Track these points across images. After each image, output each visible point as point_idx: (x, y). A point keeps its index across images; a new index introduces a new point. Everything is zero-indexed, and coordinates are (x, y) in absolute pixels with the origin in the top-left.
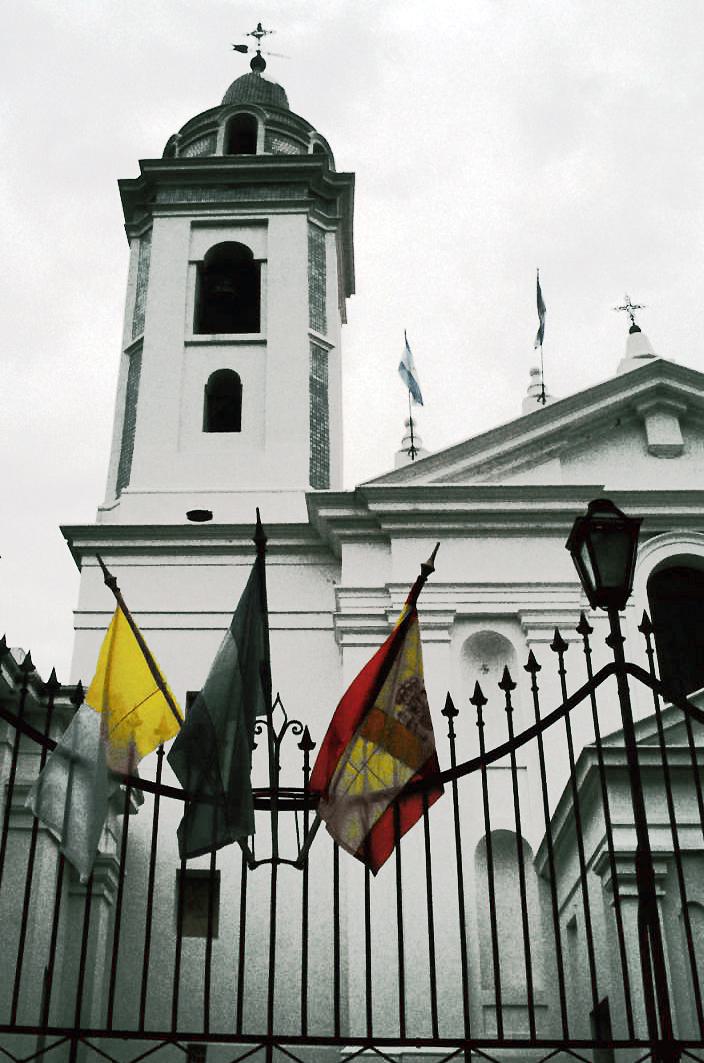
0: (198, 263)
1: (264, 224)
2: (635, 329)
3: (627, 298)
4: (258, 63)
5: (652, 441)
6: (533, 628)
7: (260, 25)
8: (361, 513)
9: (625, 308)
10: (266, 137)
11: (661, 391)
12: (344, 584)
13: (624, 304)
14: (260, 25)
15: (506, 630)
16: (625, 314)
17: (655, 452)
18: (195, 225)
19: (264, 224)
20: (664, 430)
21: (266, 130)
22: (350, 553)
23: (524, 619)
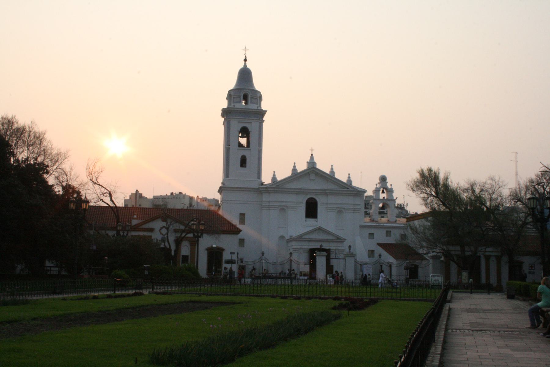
0: (239, 131)
2: (312, 155)
3: (312, 148)
4: (245, 60)
6: (289, 208)
7: (246, 47)
8: (267, 190)
9: (310, 150)
10: (251, 99)
11: (313, 171)
12: (264, 200)
13: (311, 149)
14: (246, 47)
16: (311, 151)
17: (310, 180)
19: (251, 123)
20: (312, 176)
21: (251, 97)
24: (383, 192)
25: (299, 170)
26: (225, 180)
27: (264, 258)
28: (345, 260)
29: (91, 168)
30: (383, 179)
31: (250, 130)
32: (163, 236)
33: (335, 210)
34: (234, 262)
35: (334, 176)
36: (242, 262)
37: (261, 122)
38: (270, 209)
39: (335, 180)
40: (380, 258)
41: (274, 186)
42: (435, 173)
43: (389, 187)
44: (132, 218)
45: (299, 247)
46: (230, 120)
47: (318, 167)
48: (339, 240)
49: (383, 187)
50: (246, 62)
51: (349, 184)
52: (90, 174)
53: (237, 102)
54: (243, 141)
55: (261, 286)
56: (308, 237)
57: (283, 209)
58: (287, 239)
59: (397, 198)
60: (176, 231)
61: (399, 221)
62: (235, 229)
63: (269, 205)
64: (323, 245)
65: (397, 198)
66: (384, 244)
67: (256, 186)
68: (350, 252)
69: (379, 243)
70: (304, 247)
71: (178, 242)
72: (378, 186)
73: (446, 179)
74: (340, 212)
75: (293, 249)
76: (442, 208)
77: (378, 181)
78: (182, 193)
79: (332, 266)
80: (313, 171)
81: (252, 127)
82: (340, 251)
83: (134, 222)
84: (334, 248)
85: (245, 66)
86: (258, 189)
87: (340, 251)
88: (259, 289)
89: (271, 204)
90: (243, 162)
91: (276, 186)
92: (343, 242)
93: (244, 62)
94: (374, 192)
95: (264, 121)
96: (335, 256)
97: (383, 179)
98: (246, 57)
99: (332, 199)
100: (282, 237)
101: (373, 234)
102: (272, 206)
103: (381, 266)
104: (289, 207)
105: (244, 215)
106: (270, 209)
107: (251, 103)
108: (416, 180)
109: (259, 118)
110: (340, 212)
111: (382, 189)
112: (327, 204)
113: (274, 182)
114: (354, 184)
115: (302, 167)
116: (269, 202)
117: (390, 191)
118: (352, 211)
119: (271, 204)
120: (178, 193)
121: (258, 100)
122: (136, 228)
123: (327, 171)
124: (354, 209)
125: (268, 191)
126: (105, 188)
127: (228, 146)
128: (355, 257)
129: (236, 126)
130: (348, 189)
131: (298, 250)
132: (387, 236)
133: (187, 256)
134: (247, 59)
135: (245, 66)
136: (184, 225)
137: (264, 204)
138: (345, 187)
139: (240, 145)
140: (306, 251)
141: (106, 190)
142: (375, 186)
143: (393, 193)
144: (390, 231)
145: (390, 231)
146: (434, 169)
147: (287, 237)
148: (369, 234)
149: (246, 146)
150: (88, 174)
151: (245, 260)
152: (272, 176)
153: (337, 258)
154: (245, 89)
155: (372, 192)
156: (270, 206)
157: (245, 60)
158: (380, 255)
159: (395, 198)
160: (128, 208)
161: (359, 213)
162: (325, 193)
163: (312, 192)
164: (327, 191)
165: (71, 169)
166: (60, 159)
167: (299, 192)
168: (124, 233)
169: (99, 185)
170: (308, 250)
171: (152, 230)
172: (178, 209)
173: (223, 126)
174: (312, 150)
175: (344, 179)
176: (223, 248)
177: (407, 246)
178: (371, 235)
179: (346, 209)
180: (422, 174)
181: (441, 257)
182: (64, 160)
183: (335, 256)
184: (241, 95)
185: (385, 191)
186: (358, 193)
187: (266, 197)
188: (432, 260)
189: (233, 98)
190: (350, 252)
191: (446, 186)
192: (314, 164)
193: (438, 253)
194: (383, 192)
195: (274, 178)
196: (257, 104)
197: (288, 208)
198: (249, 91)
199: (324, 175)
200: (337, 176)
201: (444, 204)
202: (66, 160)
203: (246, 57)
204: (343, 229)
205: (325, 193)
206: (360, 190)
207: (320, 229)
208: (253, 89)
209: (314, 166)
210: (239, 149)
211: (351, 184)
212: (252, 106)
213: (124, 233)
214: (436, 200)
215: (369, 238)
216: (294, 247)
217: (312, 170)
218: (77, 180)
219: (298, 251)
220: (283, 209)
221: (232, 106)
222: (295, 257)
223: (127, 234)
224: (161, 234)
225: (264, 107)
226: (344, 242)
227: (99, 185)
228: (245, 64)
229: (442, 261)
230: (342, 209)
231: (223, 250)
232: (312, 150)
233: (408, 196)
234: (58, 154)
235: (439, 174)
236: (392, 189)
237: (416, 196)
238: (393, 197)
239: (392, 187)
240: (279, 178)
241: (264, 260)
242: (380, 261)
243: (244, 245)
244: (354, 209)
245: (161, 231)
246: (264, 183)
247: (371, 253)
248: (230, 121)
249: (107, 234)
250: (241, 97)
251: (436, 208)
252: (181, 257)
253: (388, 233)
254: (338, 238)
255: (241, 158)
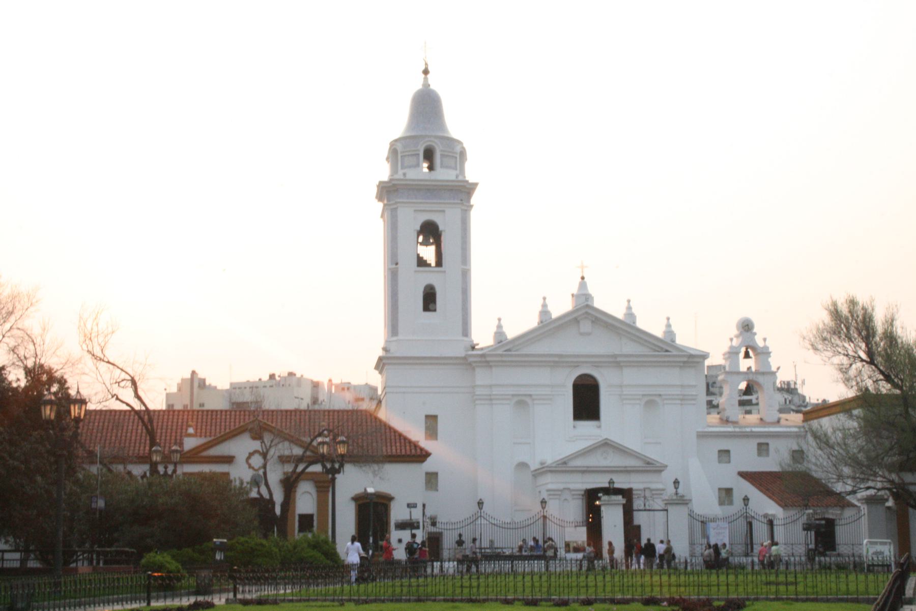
1: (444, 211)
2: (583, 278)
4: (426, 72)
5: (582, 330)
6: (536, 399)
7: (425, 43)
10: (441, 158)
11: (586, 313)
12: (478, 383)
14: (425, 43)
15: (528, 400)
17: (582, 334)
18: (415, 211)
19: (444, 211)
20: (586, 326)
21: (441, 155)
22: (478, 370)
23: (534, 397)
24: (747, 356)
25: (555, 314)
26: (390, 342)
27: (482, 514)
28: (665, 512)
29: (89, 327)
30: (747, 327)
31: (441, 228)
32: (254, 472)
33: (639, 399)
34: (415, 525)
35: (634, 323)
36: (434, 524)
37: (466, 208)
38: (494, 402)
39: (637, 334)
40: (746, 505)
41: (500, 352)
42: (864, 309)
43: (760, 344)
44: (184, 434)
45: (561, 486)
46: (395, 206)
47: (597, 304)
48: (652, 468)
49: (747, 344)
50: (429, 76)
51: (668, 340)
52: (88, 338)
53: (410, 167)
54: (428, 253)
55: (478, 578)
56: (579, 463)
57: (522, 403)
58: (532, 468)
59: (778, 368)
60: (283, 460)
61: (787, 420)
62: (416, 449)
63: (490, 395)
64: (615, 480)
65: (778, 368)
66: (755, 473)
67: (461, 353)
68: (677, 494)
69: (743, 472)
70: (572, 486)
71: (290, 484)
72: (735, 343)
73: (891, 322)
74: (651, 403)
75: (548, 490)
76: (885, 387)
77: (735, 332)
78: (295, 375)
79: (639, 527)
80: (586, 313)
81: (446, 223)
82: (654, 492)
83: (190, 443)
84: (641, 486)
85: (426, 85)
86: (465, 358)
87: (654, 492)
88: (475, 584)
89: (494, 393)
90: (429, 299)
91: (505, 351)
92: (661, 471)
93: (423, 76)
94: (727, 356)
95: (472, 206)
96: (645, 505)
97: (747, 327)
98: (426, 64)
99: (630, 376)
100: (523, 466)
101: (728, 452)
102: (497, 397)
103: (750, 524)
104: (534, 397)
105: (435, 417)
106: (492, 404)
107: (442, 166)
108: (821, 326)
109: (462, 200)
110: (651, 403)
111: (743, 350)
112: (621, 386)
113: (499, 343)
114: (680, 341)
115: (561, 306)
116: (491, 386)
117: (763, 353)
118: (679, 402)
119: (495, 391)
120: (287, 375)
121: (458, 159)
122: (194, 456)
123: (619, 313)
124: (681, 397)
125: (488, 362)
126: (122, 370)
127: (394, 266)
128: (689, 505)
129: (412, 220)
130: (667, 351)
131: (560, 493)
132: (760, 453)
133: (311, 516)
134: (430, 69)
135: (426, 85)
136: (301, 446)
137: (479, 391)
138: (659, 347)
139: (421, 262)
140: (579, 495)
141: (123, 373)
142: (729, 344)
143: (770, 356)
144: (767, 444)
145: (767, 444)
146: (862, 299)
147: (534, 466)
148: (720, 451)
149: (433, 264)
150: (82, 339)
151: (439, 520)
152: (494, 329)
153: (647, 508)
154: (426, 136)
155: (722, 357)
156: (492, 397)
157: (426, 72)
158: (746, 500)
159: (774, 369)
160: (174, 411)
161: (694, 404)
162: (616, 362)
163: (586, 362)
164: (619, 359)
165: (44, 330)
166: (18, 306)
167: (556, 362)
168: (166, 468)
169: (108, 362)
170: (583, 493)
171: (229, 460)
172: (287, 411)
173: (381, 222)
174: (582, 267)
175: (658, 331)
176: (390, 495)
177: (805, 477)
178: (724, 454)
179: (664, 397)
180: (836, 314)
181: (887, 500)
182: (27, 309)
183: (645, 505)
184: (418, 150)
185: (751, 353)
186: (691, 360)
187: (482, 377)
188: (866, 507)
189: (401, 156)
190: (677, 494)
191: (891, 338)
192: (588, 297)
193: (879, 490)
194: (747, 356)
195: (499, 334)
196: (456, 169)
197: (533, 400)
198: (436, 141)
199: (610, 321)
200: (642, 324)
201: (888, 378)
202: (31, 309)
203: (426, 64)
204: (660, 443)
205: (616, 362)
206: (692, 352)
207: (606, 445)
208: (446, 135)
209: (589, 303)
210: (419, 271)
211: (674, 341)
212: (443, 174)
213: (166, 468)
214: (869, 370)
215: (720, 462)
216: (550, 486)
217: (584, 311)
218: (58, 353)
219: (560, 495)
220: (522, 403)
221: (400, 176)
222: (553, 509)
223: (175, 471)
224: (250, 466)
225: (471, 175)
226: (663, 473)
227: (108, 362)
228: (426, 79)
229: (889, 508)
230: (657, 399)
231: (390, 499)
232: (582, 267)
233: (805, 362)
234: (14, 298)
235: (873, 309)
236: (766, 348)
237: (822, 362)
238: (770, 367)
239: (768, 344)
240: (511, 333)
241: (482, 518)
242: (746, 512)
243: (437, 485)
244: (684, 395)
245: (251, 461)
246: (478, 344)
247: (726, 494)
248: (397, 208)
249: (129, 473)
250: (418, 154)
251: (870, 388)
252: (297, 518)
253: (763, 449)
254: (648, 463)
255: (424, 292)
